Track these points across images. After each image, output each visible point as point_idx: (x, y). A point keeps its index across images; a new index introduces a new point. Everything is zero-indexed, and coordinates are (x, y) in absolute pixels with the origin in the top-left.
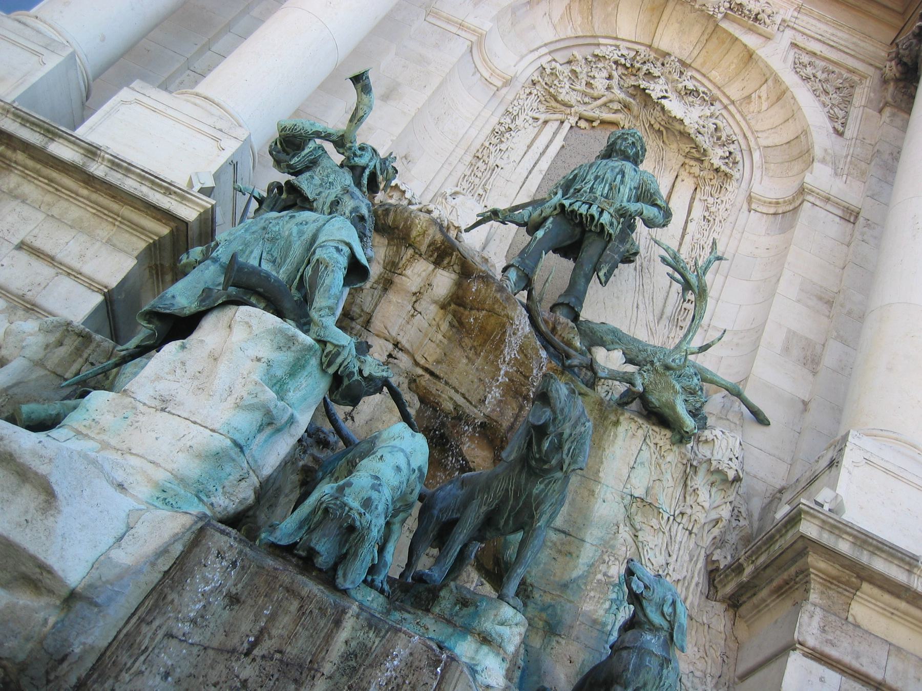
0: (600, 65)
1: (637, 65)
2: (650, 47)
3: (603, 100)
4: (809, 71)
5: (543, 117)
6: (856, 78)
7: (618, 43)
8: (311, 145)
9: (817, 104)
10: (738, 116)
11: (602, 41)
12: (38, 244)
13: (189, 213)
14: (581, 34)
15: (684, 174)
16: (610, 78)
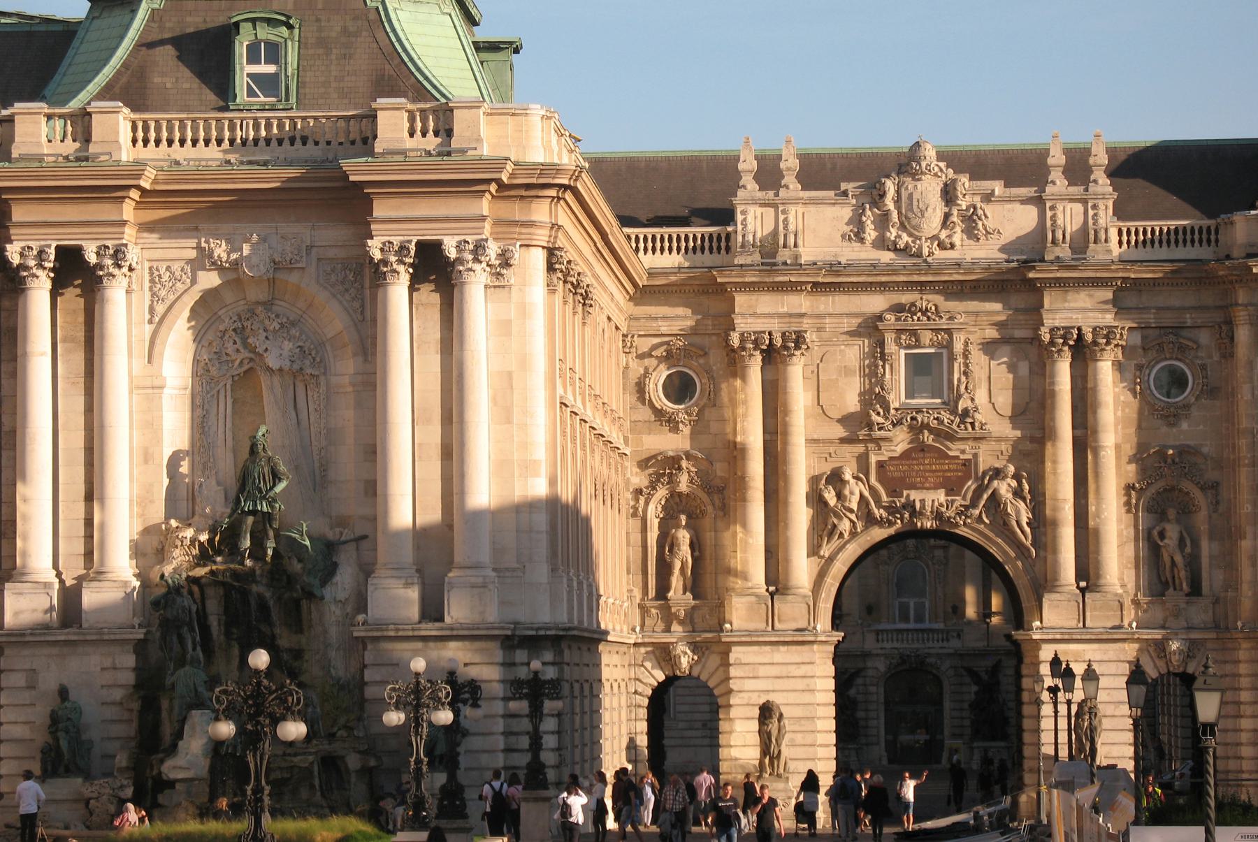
0: (227, 336)
1: (245, 324)
2: (245, 299)
3: (237, 363)
4: (333, 278)
5: (215, 392)
6: (362, 261)
7: (229, 307)
8: (163, 601)
9: (345, 303)
10: (310, 321)
11: (220, 313)
12: (105, 666)
13: (142, 636)
14: (207, 318)
15: (298, 383)
16: (235, 343)
